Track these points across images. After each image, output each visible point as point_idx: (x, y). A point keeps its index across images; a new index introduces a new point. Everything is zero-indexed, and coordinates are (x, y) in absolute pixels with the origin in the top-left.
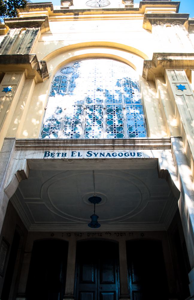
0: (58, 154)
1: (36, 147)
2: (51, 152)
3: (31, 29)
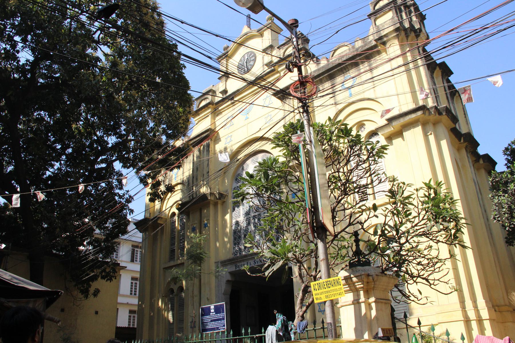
0: (241, 265)
1: (230, 263)
2: (238, 264)
3: (205, 143)
